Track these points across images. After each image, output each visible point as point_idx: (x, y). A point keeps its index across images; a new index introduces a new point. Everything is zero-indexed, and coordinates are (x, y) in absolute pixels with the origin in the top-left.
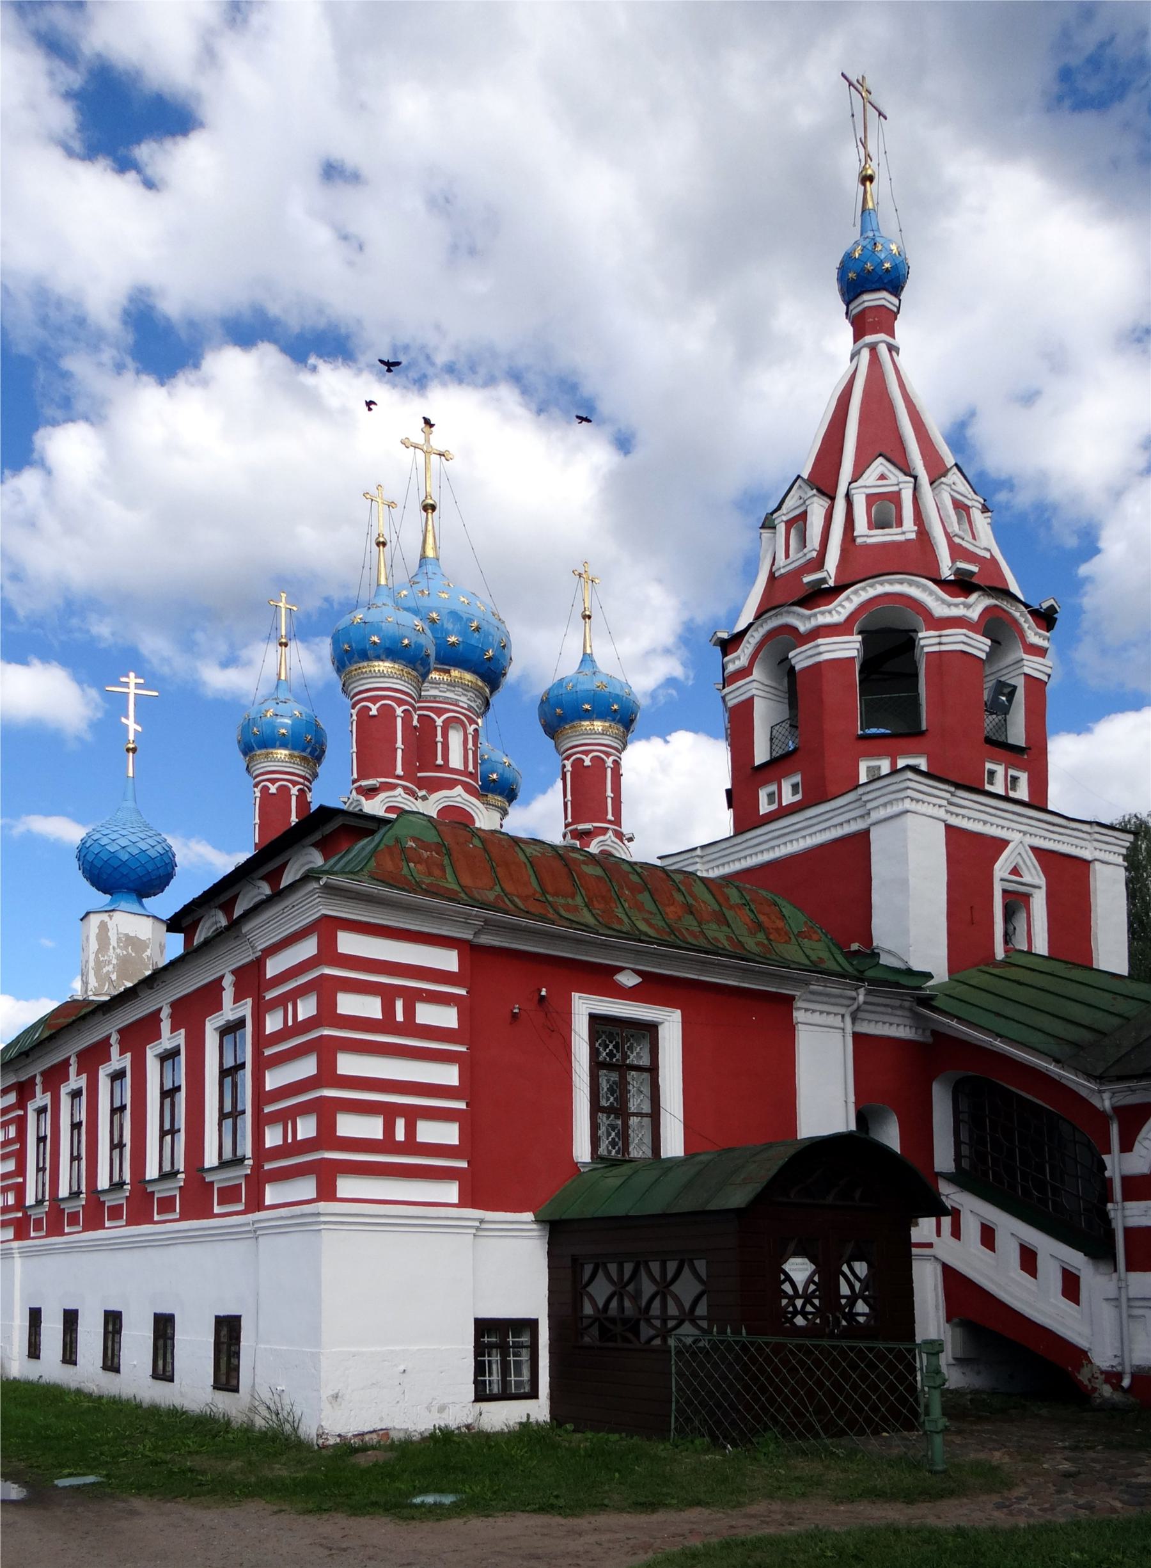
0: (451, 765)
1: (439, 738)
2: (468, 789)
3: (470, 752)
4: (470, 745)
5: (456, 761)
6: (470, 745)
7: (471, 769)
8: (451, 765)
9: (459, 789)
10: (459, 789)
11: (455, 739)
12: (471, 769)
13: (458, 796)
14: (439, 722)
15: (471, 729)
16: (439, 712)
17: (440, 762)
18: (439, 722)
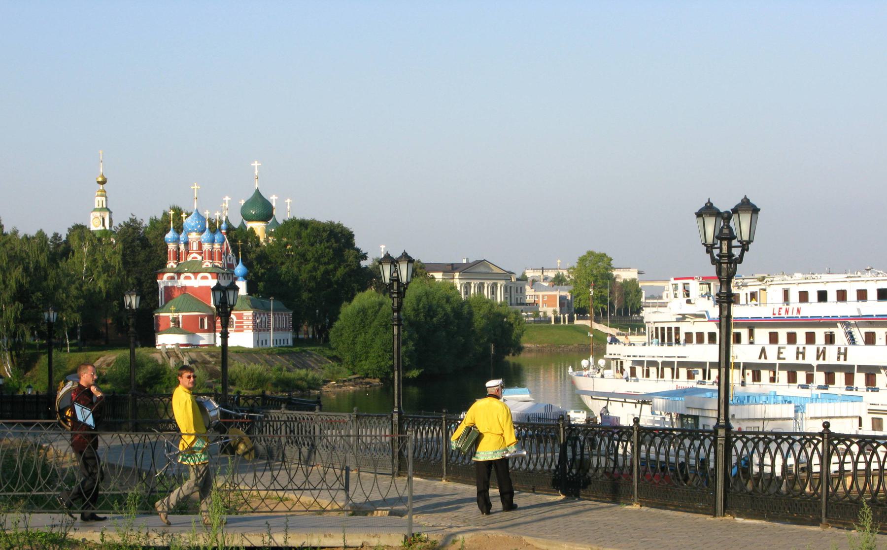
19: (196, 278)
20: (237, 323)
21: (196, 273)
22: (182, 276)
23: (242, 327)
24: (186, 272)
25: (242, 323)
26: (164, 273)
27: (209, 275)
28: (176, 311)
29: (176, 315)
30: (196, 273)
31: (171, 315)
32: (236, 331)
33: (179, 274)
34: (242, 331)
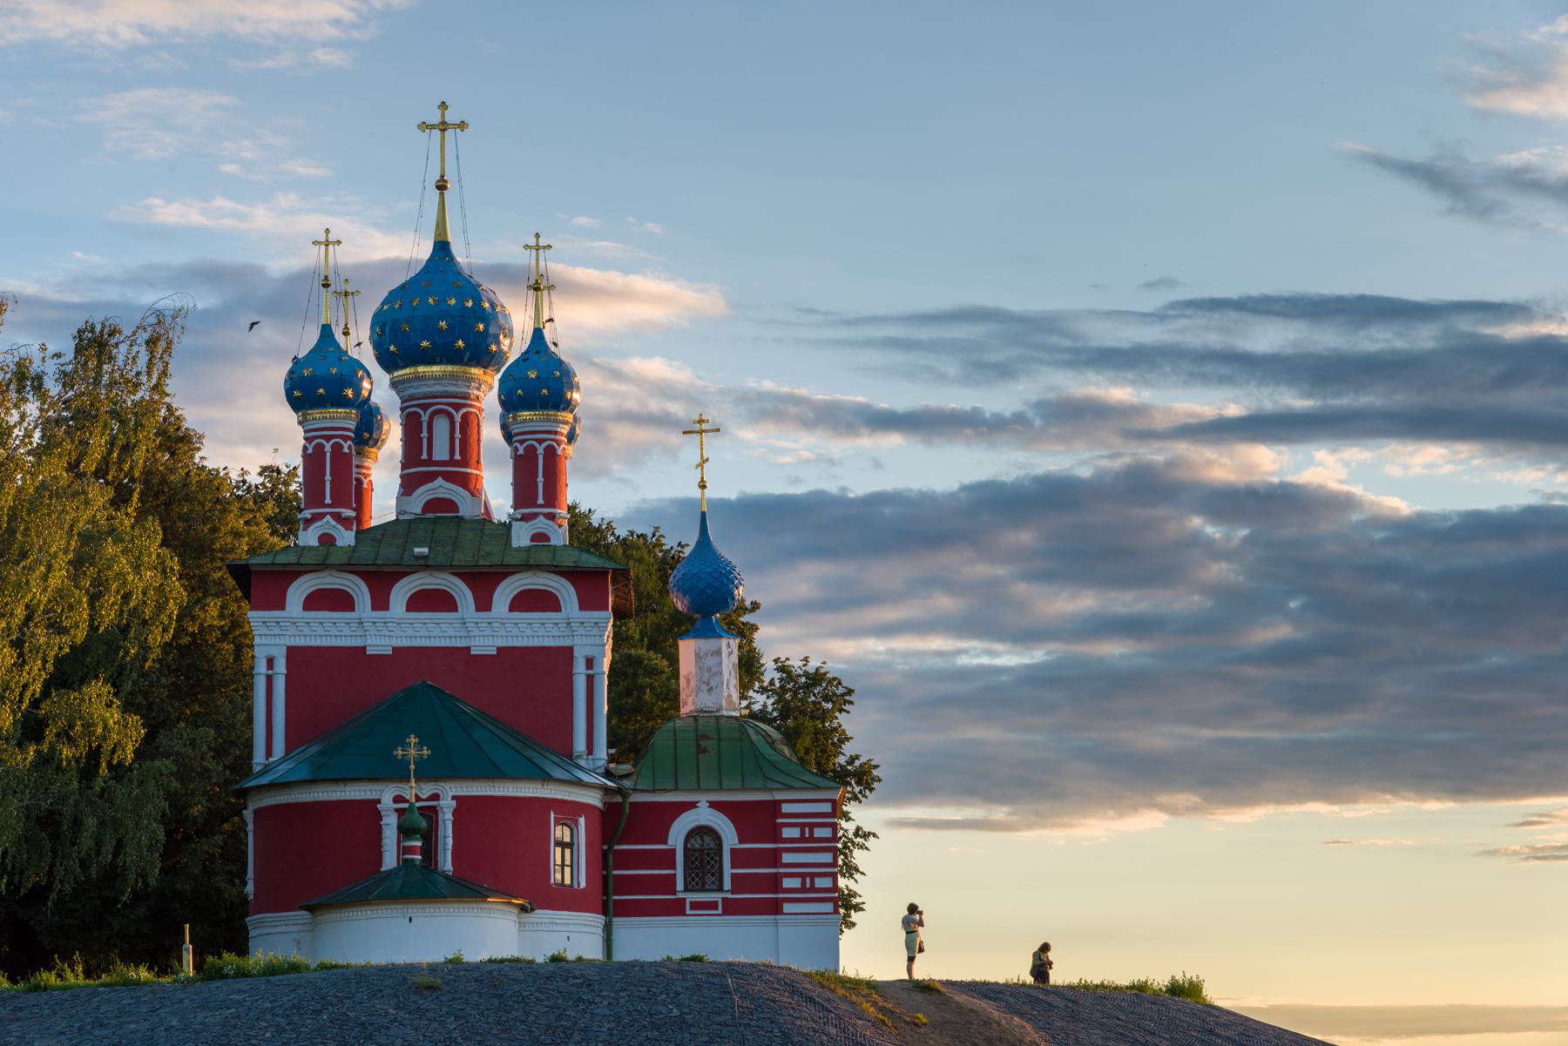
0: (437, 457)
1: (425, 434)
2: (449, 477)
3: (457, 442)
4: (458, 435)
5: (441, 453)
6: (458, 435)
7: (457, 457)
8: (437, 457)
9: (440, 481)
10: (440, 481)
11: (441, 426)
12: (457, 457)
13: (440, 488)
14: (425, 418)
15: (458, 418)
16: (425, 407)
17: (425, 456)
18: (425, 418)
19: (484, 604)
20: (738, 858)
21: (483, 582)
22: (400, 593)
23: (774, 883)
24: (424, 565)
25: (774, 858)
26: (289, 575)
27: (566, 591)
28: (427, 773)
29: (427, 790)
30: (483, 582)
31: (386, 795)
32: (731, 908)
33: (381, 582)
34: (774, 908)
